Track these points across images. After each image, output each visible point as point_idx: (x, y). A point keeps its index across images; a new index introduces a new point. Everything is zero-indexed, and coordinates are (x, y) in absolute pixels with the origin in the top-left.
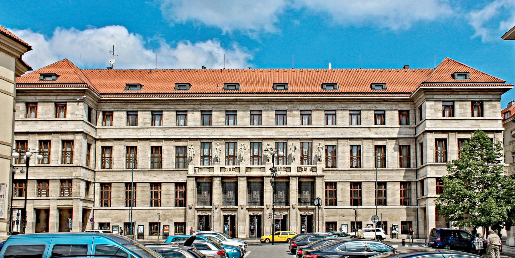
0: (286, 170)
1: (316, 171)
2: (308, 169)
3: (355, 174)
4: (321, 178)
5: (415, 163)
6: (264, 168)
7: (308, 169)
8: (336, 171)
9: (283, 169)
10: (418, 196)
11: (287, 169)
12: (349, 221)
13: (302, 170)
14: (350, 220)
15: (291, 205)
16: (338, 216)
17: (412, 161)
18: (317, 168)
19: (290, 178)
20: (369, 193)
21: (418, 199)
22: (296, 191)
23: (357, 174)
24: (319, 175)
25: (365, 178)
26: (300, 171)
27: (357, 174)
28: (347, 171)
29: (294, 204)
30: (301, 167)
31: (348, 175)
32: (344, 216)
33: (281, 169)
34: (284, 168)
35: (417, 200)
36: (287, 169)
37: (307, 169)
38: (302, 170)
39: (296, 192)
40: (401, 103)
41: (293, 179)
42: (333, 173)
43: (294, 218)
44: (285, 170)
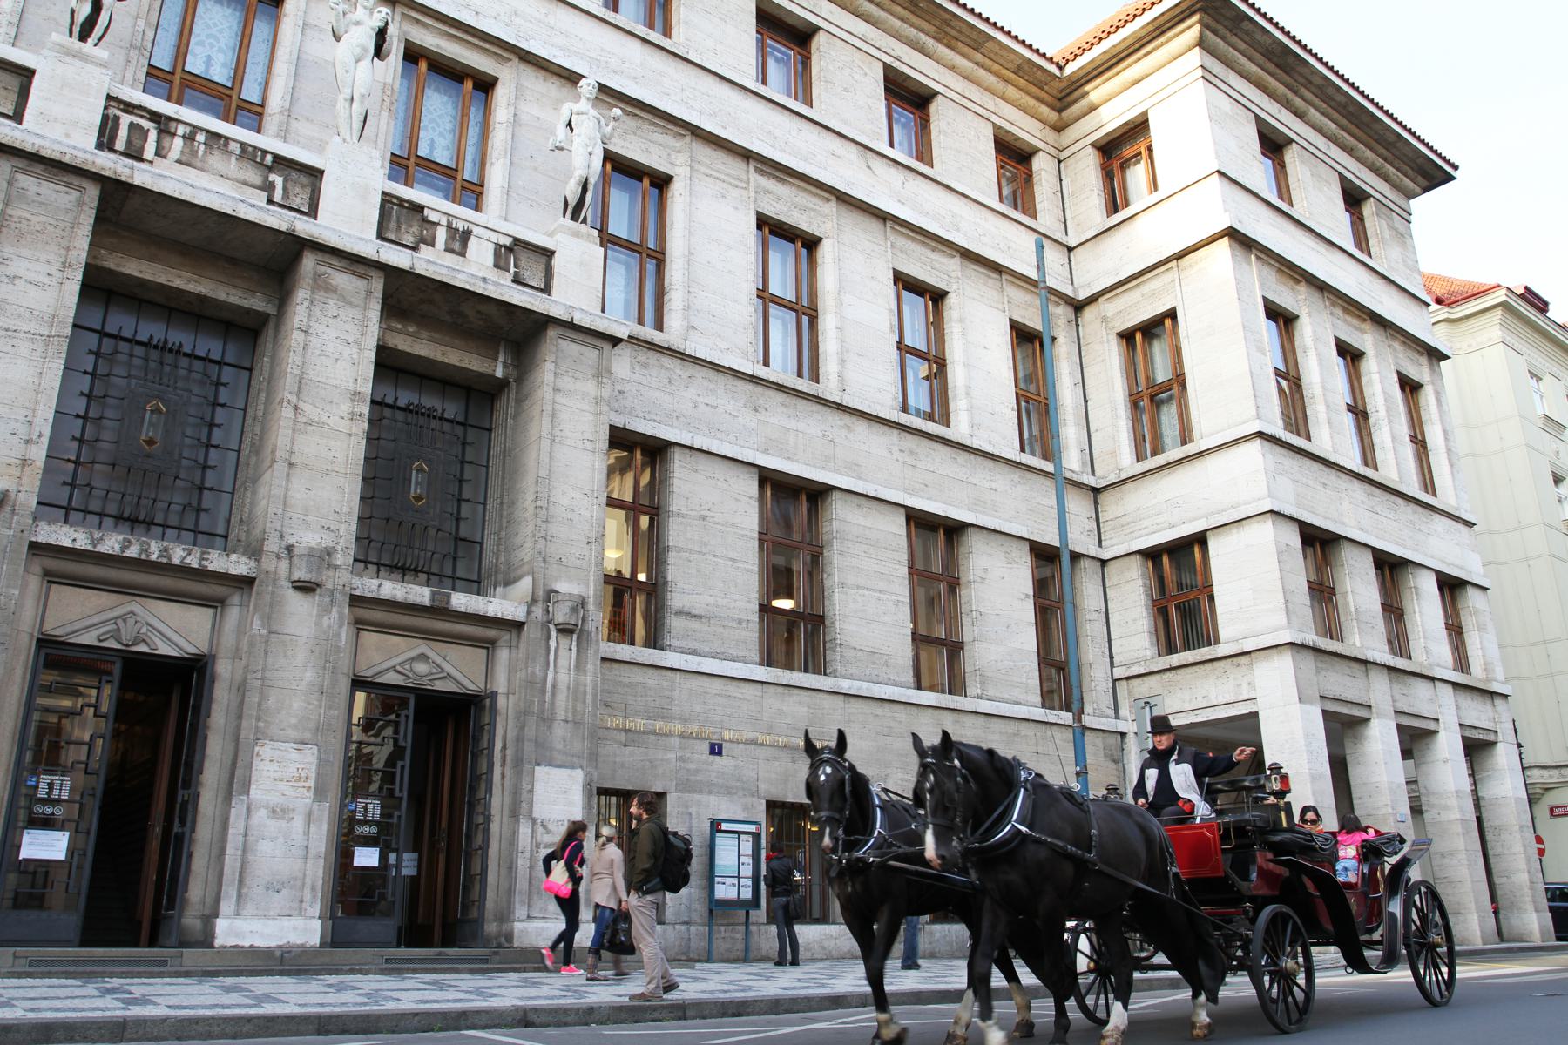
0: (269, 187)
1: (547, 289)
2: (480, 253)
3: (792, 424)
4: (590, 355)
5: (1088, 451)
6: (14, 82)
7: (480, 253)
8: (666, 361)
9: (233, 166)
10: (1116, 660)
11: (278, 180)
12: (756, 793)
13: (432, 245)
14: (763, 787)
15: (272, 545)
16: (675, 741)
17: (1070, 434)
18: (557, 262)
19: (309, 262)
20: (881, 585)
21: (1118, 673)
22: (345, 408)
23: (801, 426)
24: (579, 319)
25: (853, 468)
26: (409, 239)
27: (801, 426)
28: (742, 386)
29: (308, 538)
30: (418, 208)
31: (747, 418)
32: (716, 750)
33: (216, 160)
34: (249, 153)
35: (1114, 681)
36: (278, 180)
37: (473, 241)
38: (432, 245)
39: (345, 425)
40: (1011, 92)
41: (330, 289)
42: (645, 366)
43: (297, 704)
44: (254, 176)
